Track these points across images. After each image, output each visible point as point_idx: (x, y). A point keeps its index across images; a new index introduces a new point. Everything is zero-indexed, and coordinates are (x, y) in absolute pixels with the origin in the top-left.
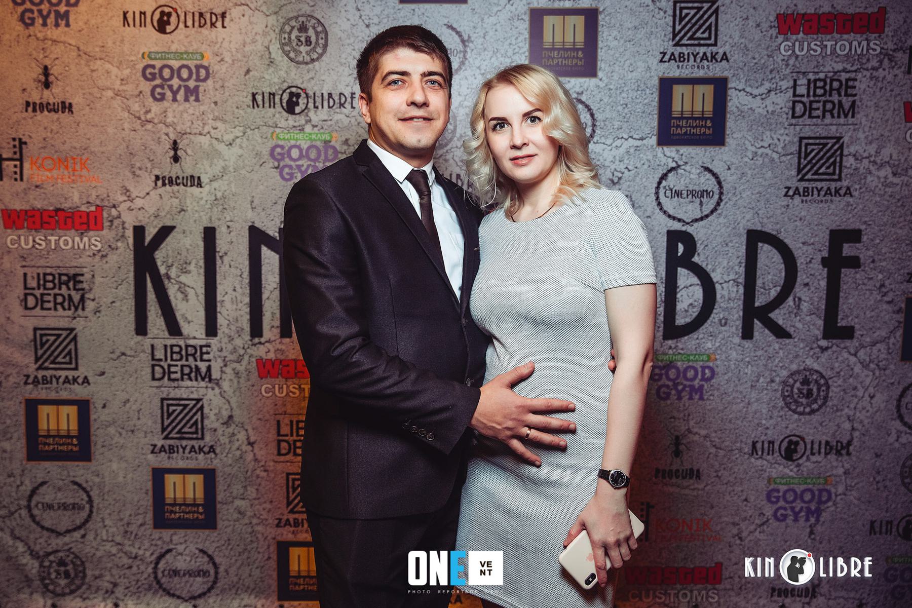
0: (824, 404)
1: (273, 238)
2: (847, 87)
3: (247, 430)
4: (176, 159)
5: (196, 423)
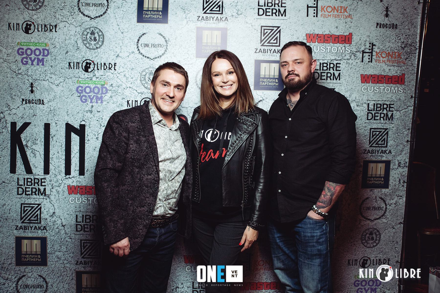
1: (77, 129)
2: (337, 67)
4: (32, 91)
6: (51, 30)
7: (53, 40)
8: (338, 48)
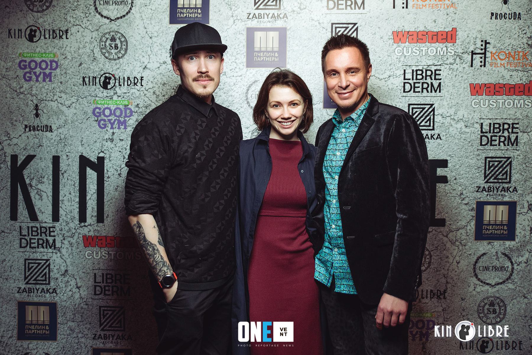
0: (429, 267)
2: (436, 75)
3: (76, 279)
4: (37, 115)
5: (45, 274)
6: (61, 37)
7: (64, 49)
8: (437, 49)
